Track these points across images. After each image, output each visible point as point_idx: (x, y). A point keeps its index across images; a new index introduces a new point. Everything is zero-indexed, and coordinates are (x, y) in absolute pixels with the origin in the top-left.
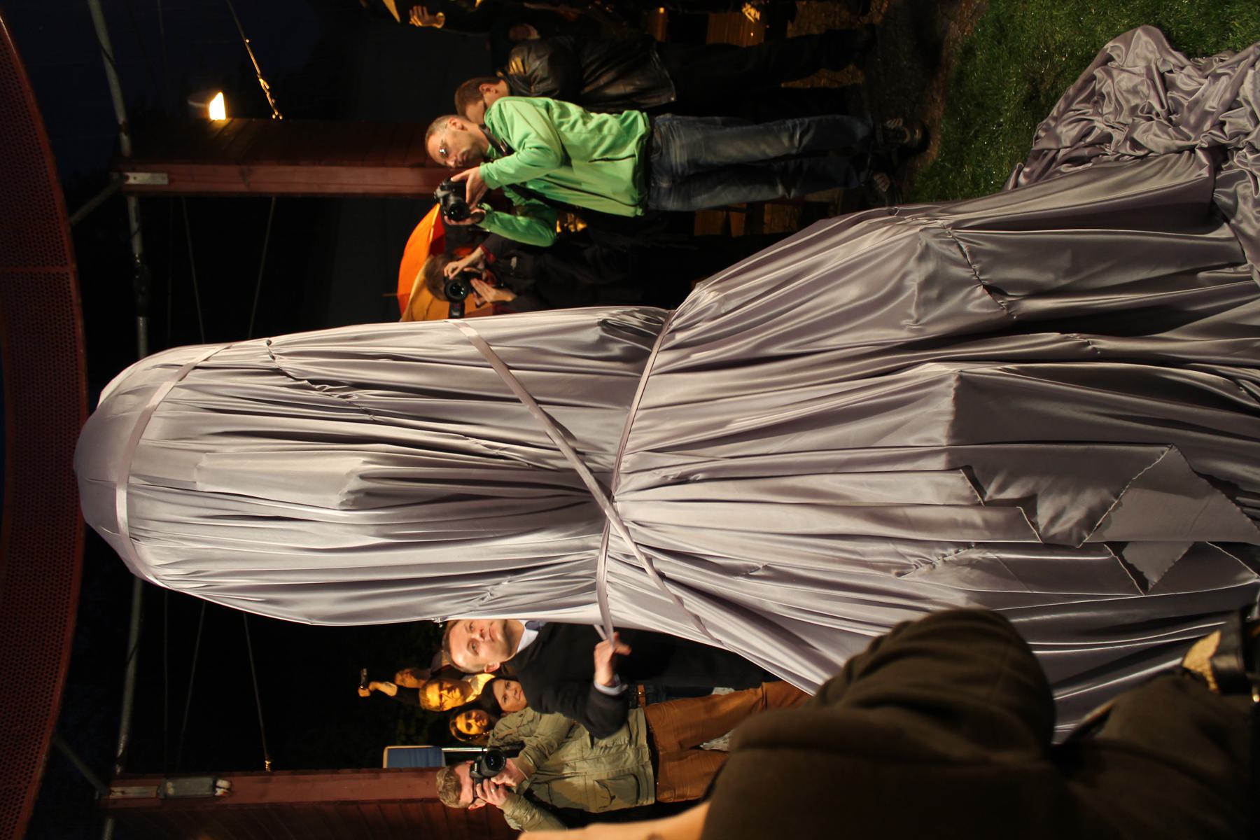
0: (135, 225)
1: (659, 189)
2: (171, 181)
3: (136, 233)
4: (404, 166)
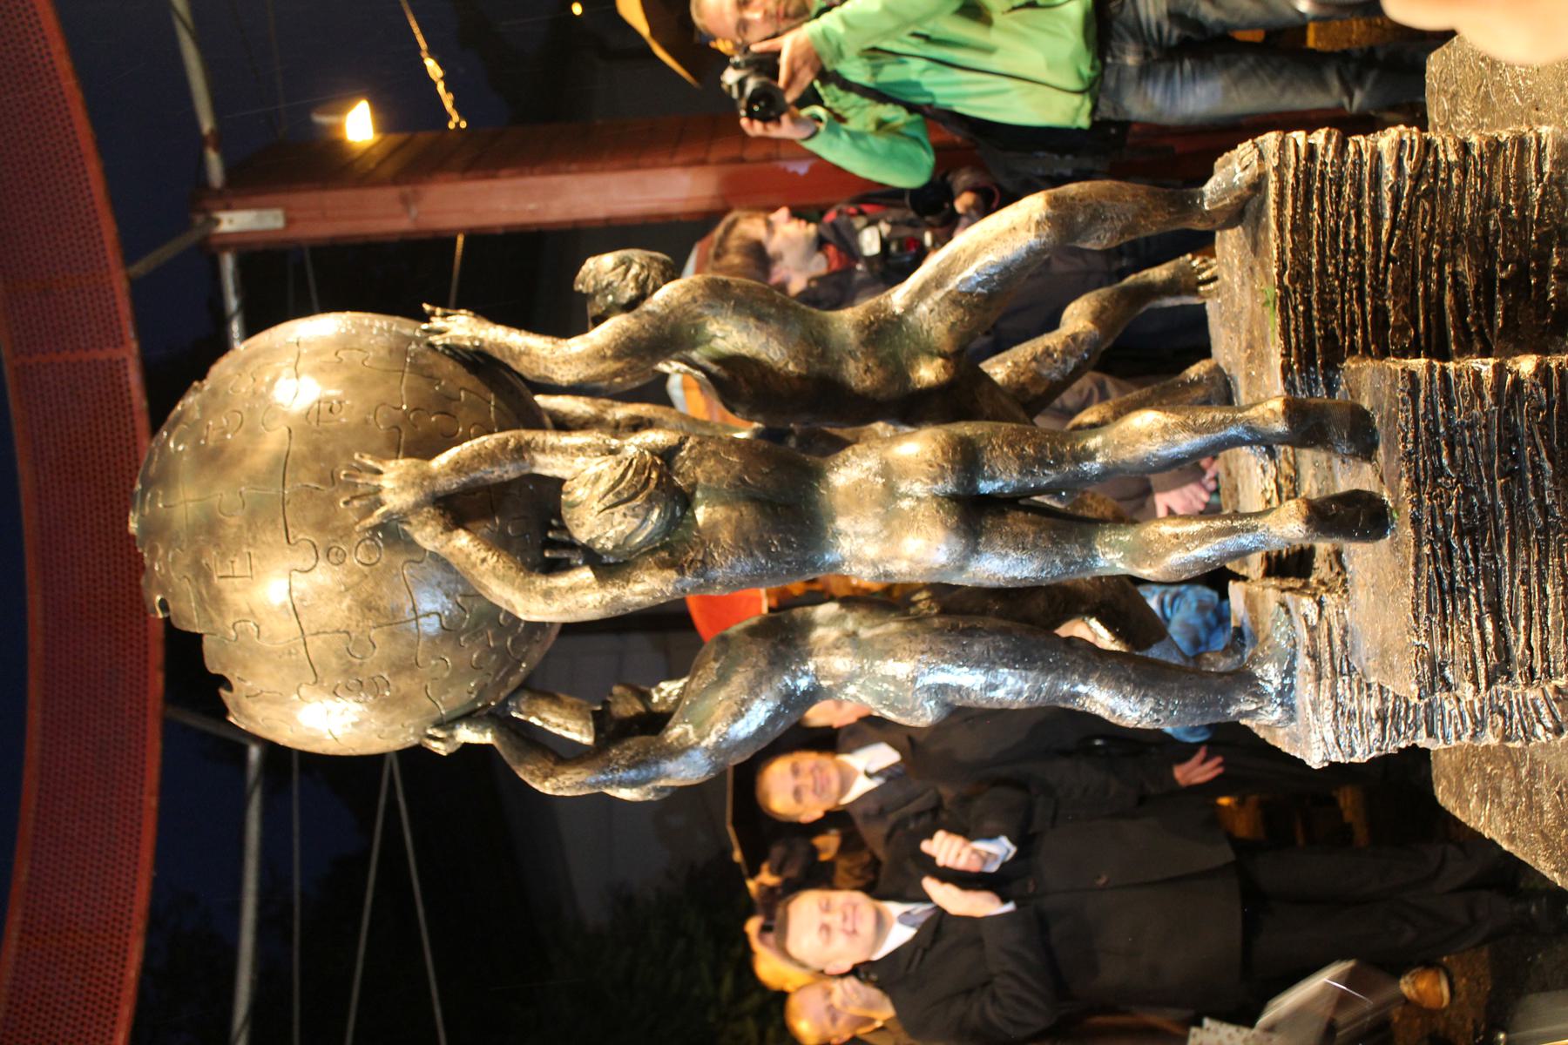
0: (233, 303)
1: (1122, 68)
2: (289, 221)
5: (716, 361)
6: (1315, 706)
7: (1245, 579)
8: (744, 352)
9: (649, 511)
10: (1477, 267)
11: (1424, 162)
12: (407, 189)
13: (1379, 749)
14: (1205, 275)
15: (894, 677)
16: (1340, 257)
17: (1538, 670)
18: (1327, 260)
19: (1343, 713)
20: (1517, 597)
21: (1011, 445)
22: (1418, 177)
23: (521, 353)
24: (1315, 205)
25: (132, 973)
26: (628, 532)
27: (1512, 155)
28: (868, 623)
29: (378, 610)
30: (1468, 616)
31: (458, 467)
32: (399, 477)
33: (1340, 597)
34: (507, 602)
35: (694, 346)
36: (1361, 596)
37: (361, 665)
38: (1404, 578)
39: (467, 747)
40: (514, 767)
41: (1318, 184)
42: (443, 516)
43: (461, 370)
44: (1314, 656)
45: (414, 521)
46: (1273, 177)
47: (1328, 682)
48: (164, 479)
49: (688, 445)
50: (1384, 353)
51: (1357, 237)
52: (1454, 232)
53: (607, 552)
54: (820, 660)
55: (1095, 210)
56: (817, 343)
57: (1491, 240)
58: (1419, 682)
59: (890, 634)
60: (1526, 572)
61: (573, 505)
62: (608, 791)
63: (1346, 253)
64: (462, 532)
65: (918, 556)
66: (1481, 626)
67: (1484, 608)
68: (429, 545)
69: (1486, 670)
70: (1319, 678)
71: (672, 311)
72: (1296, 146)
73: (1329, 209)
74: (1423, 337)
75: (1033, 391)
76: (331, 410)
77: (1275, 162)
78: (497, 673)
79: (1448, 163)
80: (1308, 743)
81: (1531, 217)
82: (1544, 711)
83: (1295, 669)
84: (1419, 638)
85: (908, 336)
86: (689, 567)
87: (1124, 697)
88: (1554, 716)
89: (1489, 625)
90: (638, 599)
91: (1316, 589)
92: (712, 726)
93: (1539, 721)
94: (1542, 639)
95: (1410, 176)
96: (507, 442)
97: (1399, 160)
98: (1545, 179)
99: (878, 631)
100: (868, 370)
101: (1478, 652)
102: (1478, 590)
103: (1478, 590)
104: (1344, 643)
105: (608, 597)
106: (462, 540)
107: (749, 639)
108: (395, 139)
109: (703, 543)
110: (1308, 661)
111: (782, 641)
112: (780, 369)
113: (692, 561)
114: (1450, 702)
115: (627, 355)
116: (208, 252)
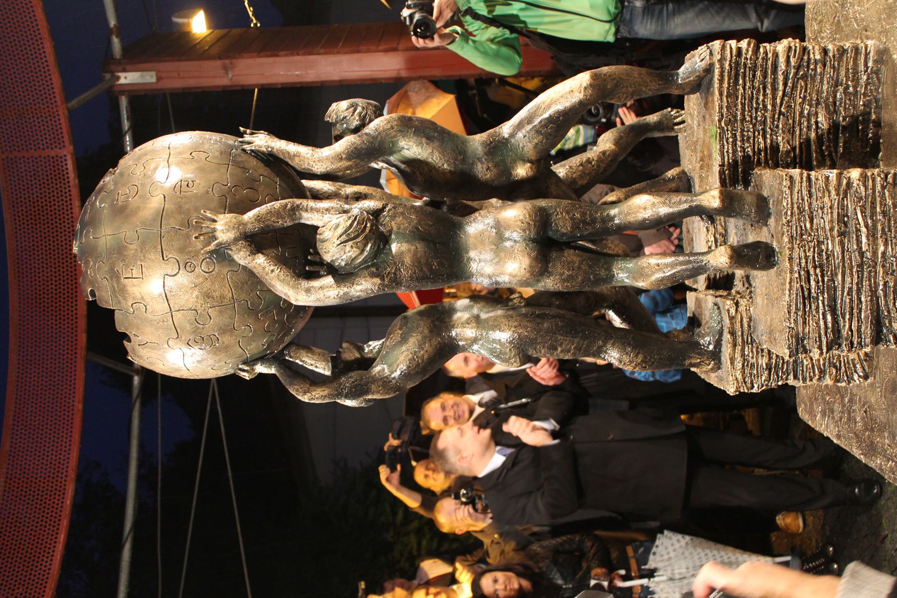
0: (126, 125)
2: (159, 79)
3: (126, 133)
4: (379, 51)
5: (403, 162)
6: (732, 360)
7: (695, 290)
8: (419, 157)
9: (365, 245)
10: (829, 119)
11: (802, 59)
12: (227, 61)
13: (767, 385)
14: (678, 120)
15: (500, 340)
16: (754, 111)
17: (855, 343)
18: (746, 113)
19: (747, 365)
20: (845, 302)
21: (568, 213)
22: (798, 68)
23: (295, 156)
24: (741, 82)
25: (68, 502)
26: (353, 256)
27: (851, 57)
28: (485, 310)
29: (213, 298)
30: (818, 312)
31: (258, 218)
32: (226, 224)
33: (748, 301)
34: (285, 294)
35: (391, 154)
36: (759, 300)
37: (203, 328)
38: (783, 290)
39: (260, 375)
40: (287, 387)
41: (742, 70)
42: (250, 246)
43: (261, 165)
44: (732, 333)
45: (234, 249)
46: (717, 65)
47: (740, 348)
48: (93, 223)
49: (387, 209)
50: (776, 166)
51: (763, 101)
52: (817, 99)
53: (341, 267)
54: (458, 330)
55: (617, 82)
56: (461, 154)
57: (838, 103)
58: (789, 348)
59: (498, 317)
60: (850, 289)
61: (323, 241)
62: (339, 401)
63: (757, 109)
64: (260, 255)
65: (514, 273)
66: (824, 318)
67: (826, 308)
68: (242, 262)
69: (827, 342)
70: (735, 346)
71: (379, 134)
72: (731, 48)
73: (748, 84)
74: (798, 157)
75: (580, 183)
76: (187, 186)
77: (719, 57)
78: (278, 335)
79: (815, 60)
80: (728, 381)
81: (860, 92)
82: (858, 366)
83: (722, 340)
84: (790, 323)
85: (511, 150)
86: (387, 277)
87: (627, 353)
88: (864, 369)
89: (829, 318)
90: (358, 294)
91: (735, 296)
92: (398, 366)
93: (856, 372)
94: (858, 326)
95: (794, 67)
96: (286, 205)
97: (788, 57)
98: (869, 70)
99: (492, 314)
100: (488, 169)
101: (822, 332)
102: (824, 298)
103: (824, 298)
104: (749, 326)
105: (342, 294)
106: (261, 259)
107: (419, 318)
108: (219, 32)
109: (395, 263)
110: (729, 336)
111: (437, 319)
112: (439, 167)
113: (389, 273)
114: (807, 360)
115: (354, 158)
116: (112, 96)
